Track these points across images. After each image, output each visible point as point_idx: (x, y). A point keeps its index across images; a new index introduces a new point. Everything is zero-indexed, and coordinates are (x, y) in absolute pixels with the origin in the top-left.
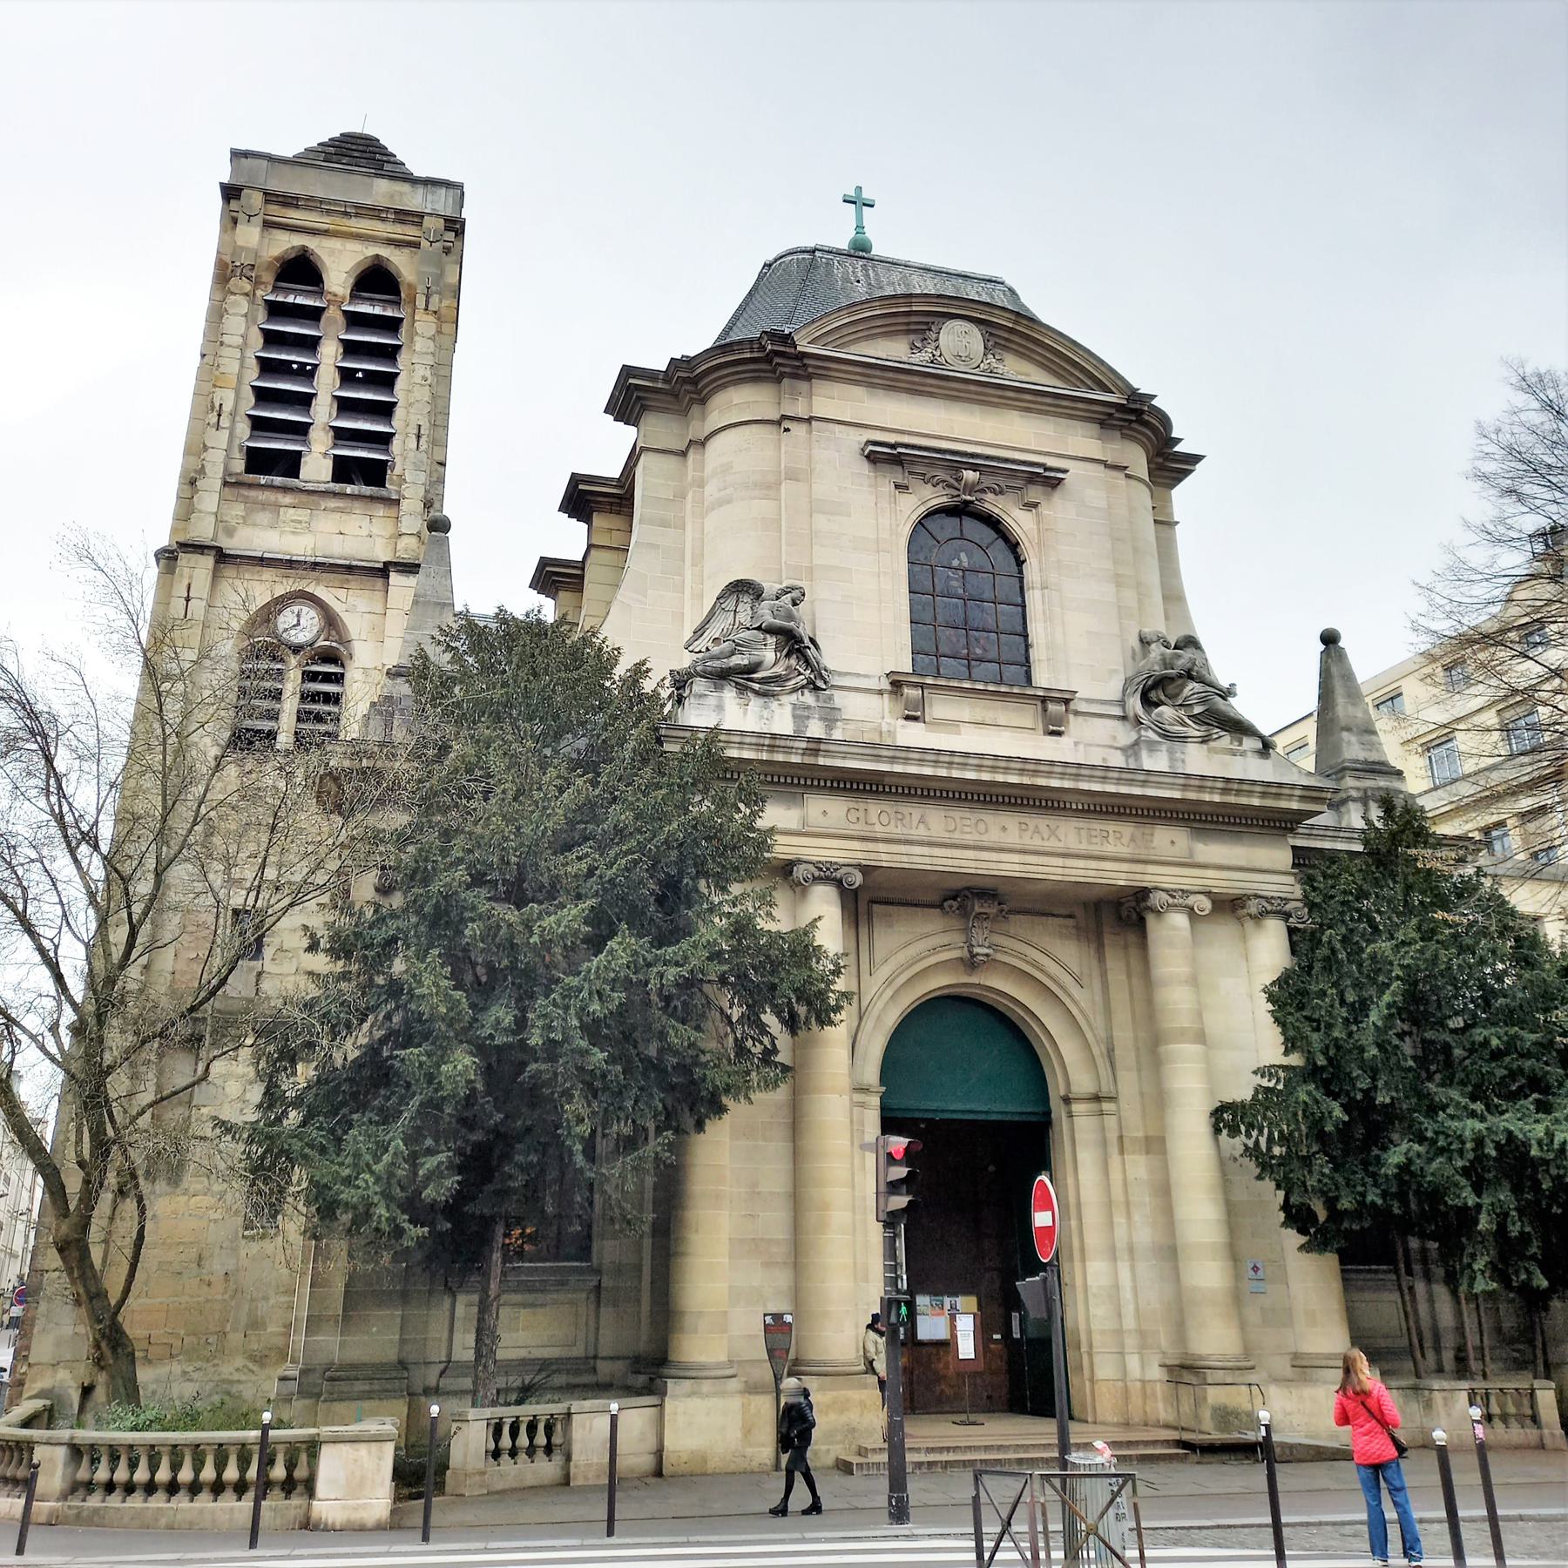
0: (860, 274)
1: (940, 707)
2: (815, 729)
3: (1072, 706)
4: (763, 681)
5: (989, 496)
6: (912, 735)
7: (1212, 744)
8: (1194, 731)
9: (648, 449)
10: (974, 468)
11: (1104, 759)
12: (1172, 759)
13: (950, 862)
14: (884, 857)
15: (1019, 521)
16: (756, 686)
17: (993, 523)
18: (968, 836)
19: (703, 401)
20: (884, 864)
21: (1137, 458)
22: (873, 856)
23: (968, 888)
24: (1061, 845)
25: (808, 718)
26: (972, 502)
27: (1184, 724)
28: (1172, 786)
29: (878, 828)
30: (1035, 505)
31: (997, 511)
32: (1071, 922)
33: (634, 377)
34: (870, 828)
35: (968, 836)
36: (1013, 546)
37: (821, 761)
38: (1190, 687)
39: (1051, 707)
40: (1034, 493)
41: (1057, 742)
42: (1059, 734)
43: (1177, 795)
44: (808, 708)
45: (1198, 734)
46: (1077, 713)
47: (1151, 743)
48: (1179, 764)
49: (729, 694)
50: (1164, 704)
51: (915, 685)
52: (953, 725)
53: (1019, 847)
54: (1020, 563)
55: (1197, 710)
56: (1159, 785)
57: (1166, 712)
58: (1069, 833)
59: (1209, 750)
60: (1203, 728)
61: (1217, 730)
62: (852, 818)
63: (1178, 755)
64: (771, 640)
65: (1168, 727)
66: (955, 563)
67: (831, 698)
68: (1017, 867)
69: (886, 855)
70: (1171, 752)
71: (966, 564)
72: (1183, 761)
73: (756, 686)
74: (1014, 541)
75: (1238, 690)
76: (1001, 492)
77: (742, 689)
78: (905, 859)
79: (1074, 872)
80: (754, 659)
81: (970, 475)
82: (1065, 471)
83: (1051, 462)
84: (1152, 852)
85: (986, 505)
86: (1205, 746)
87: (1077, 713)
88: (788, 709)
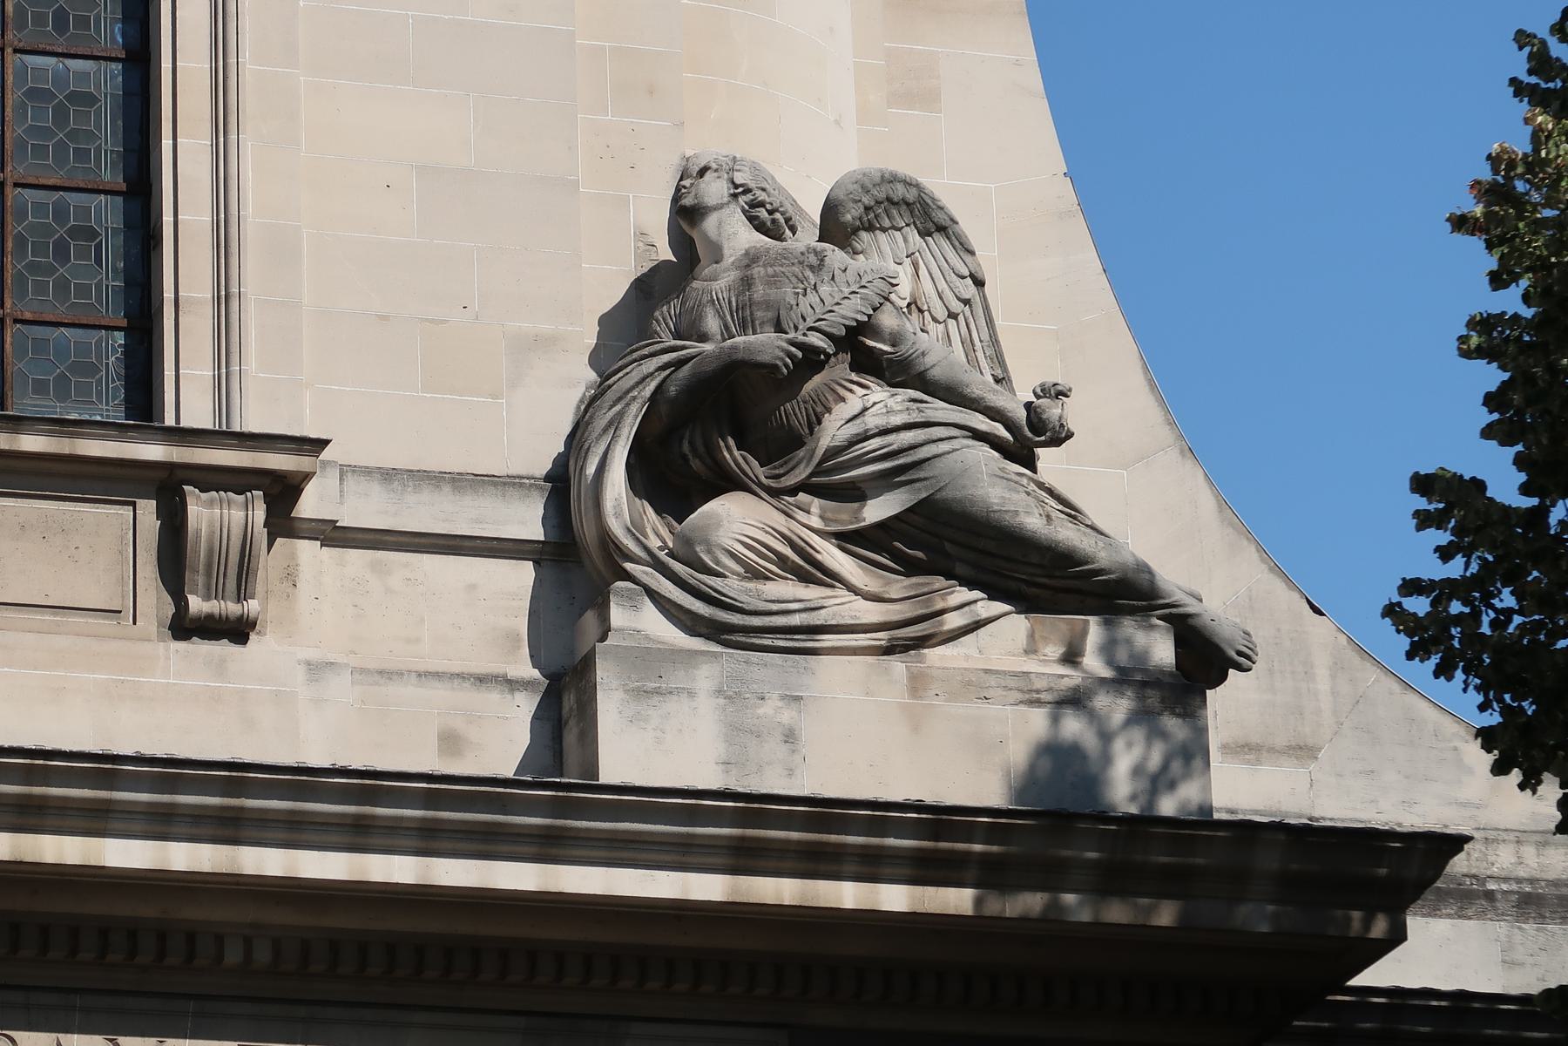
3: (309, 506)
7: (935, 656)
11: (450, 741)
12: (738, 732)
27: (812, 572)
28: (683, 856)
38: (853, 403)
39: (203, 512)
41: (220, 669)
42: (238, 631)
45: (871, 613)
46: (333, 535)
47: (649, 658)
48: (774, 748)
50: (726, 482)
55: (877, 510)
59: (917, 684)
60: (899, 586)
61: (962, 594)
63: (772, 710)
65: (733, 586)
70: (730, 694)
72: (790, 737)
75: (1072, 394)
86: (898, 666)
87: (333, 535)
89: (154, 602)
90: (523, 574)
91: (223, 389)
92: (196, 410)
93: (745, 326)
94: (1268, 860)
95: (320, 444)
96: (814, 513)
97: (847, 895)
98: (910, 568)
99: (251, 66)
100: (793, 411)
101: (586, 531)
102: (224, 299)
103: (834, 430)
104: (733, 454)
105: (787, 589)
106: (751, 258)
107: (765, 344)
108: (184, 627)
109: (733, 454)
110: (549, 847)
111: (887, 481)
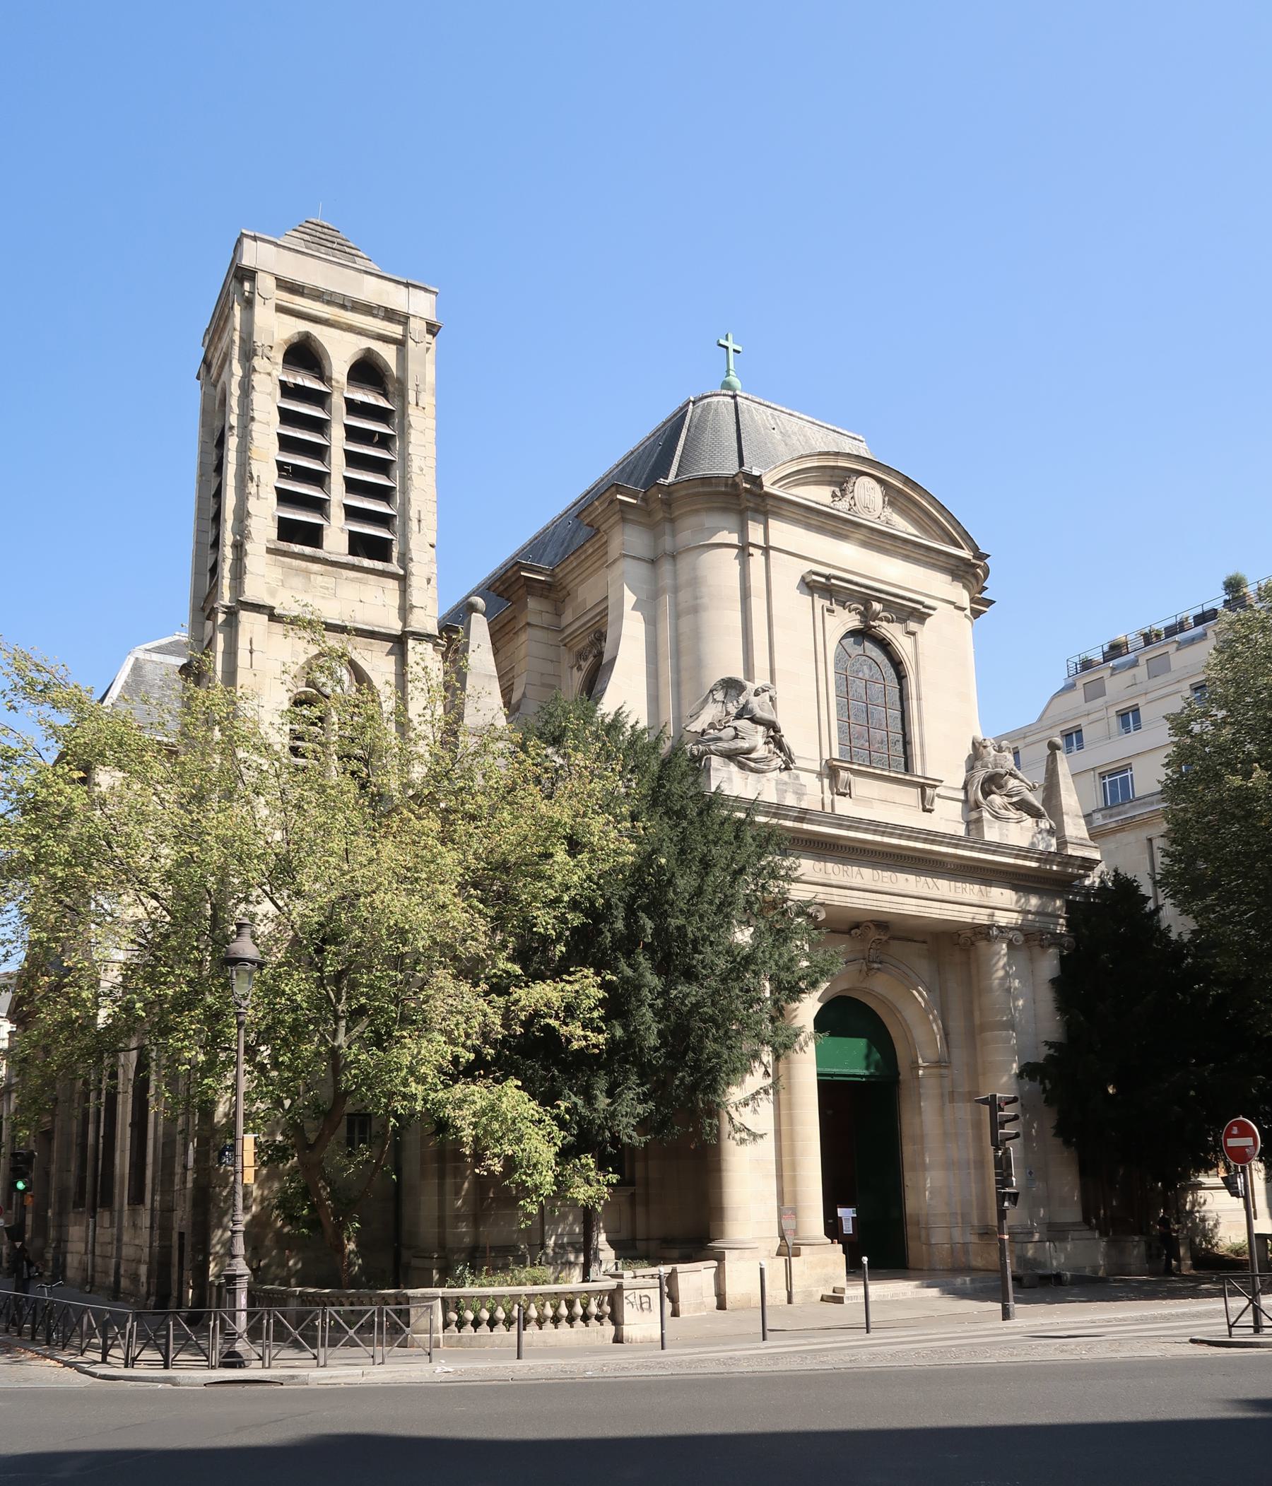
0: (772, 422)
1: (861, 787)
2: (790, 800)
4: (754, 760)
5: (884, 624)
6: (844, 807)
8: (1013, 814)
9: (625, 556)
10: (879, 600)
12: (1001, 835)
13: (875, 903)
14: (836, 898)
15: (903, 644)
16: (752, 764)
17: (884, 645)
18: (886, 885)
19: (672, 521)
20: (836, 903)
21: (964, 597)
22: (829, 897)
23: (871, 921)
24: (939, 892)
25: (786, 791)
26: (875, 627)
27: (1007, 809)
28: (1009, 855)
29: (832, 876)
30: (913, 634)
31: (889, 636)
32: (925, 946)
33: (621, 494)
34: (826, 876)
35: (886, 885)
36: (897, 664)
37: (805, 826)
40: (913, 626)
42: (930, 811)
43: (1011, 861)
44: (786, 783)
45: (1016, 817)
49: (733, 768)
50: (994, 793)
51: (846, 769)
52: (867, 801)
53: (916, 894)
54: (901, 677)
55: (1015, 799)
56: (1003, 854)
57: (997, 799)
58: (944, 887)
62: (817, 870)
64: (761, 729)
66: (861, 675)
67: (797, 777)
68: (914, 908)
69: (838, 898)
70: (1000, 828)
71: (867, 677)
73: (752, 764)
74: (897, 660)
76: (893, 622)
77: (742, 766)
78: (848, 900)
79: (946, 912)
80: (753, 744)
81: (877, 606)
82: (934, 609)
83: (928, 601)
84: (991, 900)
85: (883, 630)
87: (939, 796)
88: (773, 783)
89: (921, 806)
90: (960, 804)
91: (923, 769)
92: (919, 774)
93: (996, 767)
94: (1078, 862)
95: (942, 781)
96: (1006, 799)
97: (1028, 863)
98: (1018, 809)
99: (925, 716)
100: (1003, 782)
101: (972, 799)
102: (923, 755)
103: (1010, 786)
104: (994, 788)
105: (1003, 811)
106: (995, 756)
107: (999, 770)
108: (925, 810)
109: (994, 788)
110: (972, 849)
111: (1016, 795)
